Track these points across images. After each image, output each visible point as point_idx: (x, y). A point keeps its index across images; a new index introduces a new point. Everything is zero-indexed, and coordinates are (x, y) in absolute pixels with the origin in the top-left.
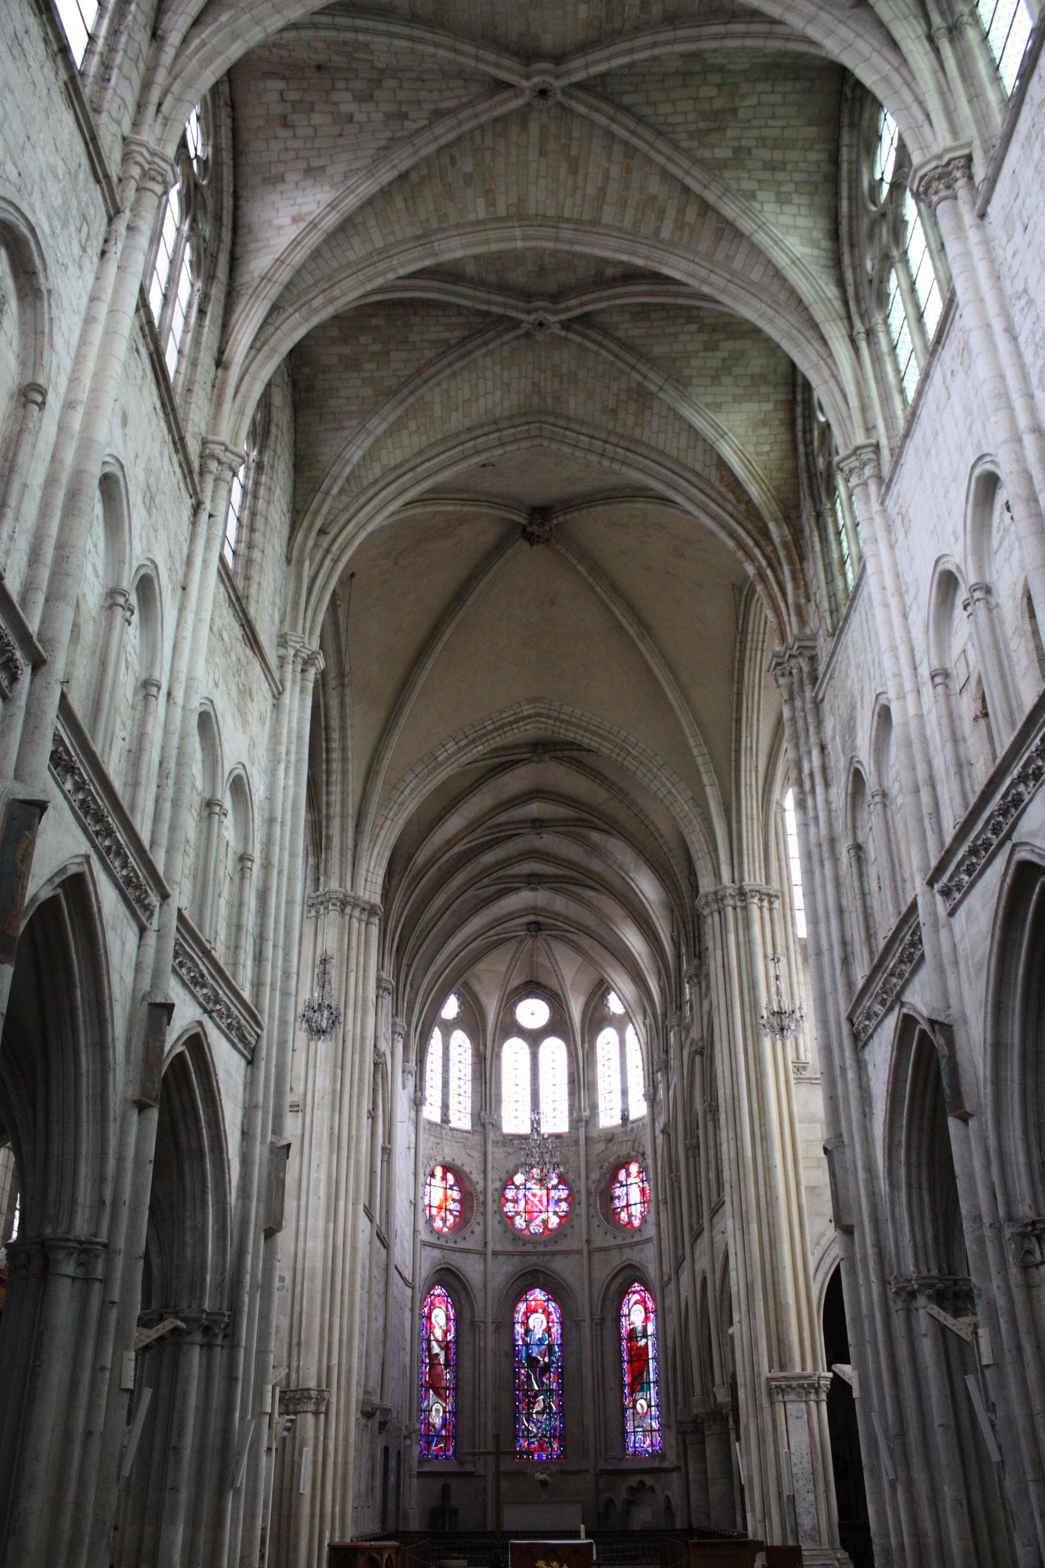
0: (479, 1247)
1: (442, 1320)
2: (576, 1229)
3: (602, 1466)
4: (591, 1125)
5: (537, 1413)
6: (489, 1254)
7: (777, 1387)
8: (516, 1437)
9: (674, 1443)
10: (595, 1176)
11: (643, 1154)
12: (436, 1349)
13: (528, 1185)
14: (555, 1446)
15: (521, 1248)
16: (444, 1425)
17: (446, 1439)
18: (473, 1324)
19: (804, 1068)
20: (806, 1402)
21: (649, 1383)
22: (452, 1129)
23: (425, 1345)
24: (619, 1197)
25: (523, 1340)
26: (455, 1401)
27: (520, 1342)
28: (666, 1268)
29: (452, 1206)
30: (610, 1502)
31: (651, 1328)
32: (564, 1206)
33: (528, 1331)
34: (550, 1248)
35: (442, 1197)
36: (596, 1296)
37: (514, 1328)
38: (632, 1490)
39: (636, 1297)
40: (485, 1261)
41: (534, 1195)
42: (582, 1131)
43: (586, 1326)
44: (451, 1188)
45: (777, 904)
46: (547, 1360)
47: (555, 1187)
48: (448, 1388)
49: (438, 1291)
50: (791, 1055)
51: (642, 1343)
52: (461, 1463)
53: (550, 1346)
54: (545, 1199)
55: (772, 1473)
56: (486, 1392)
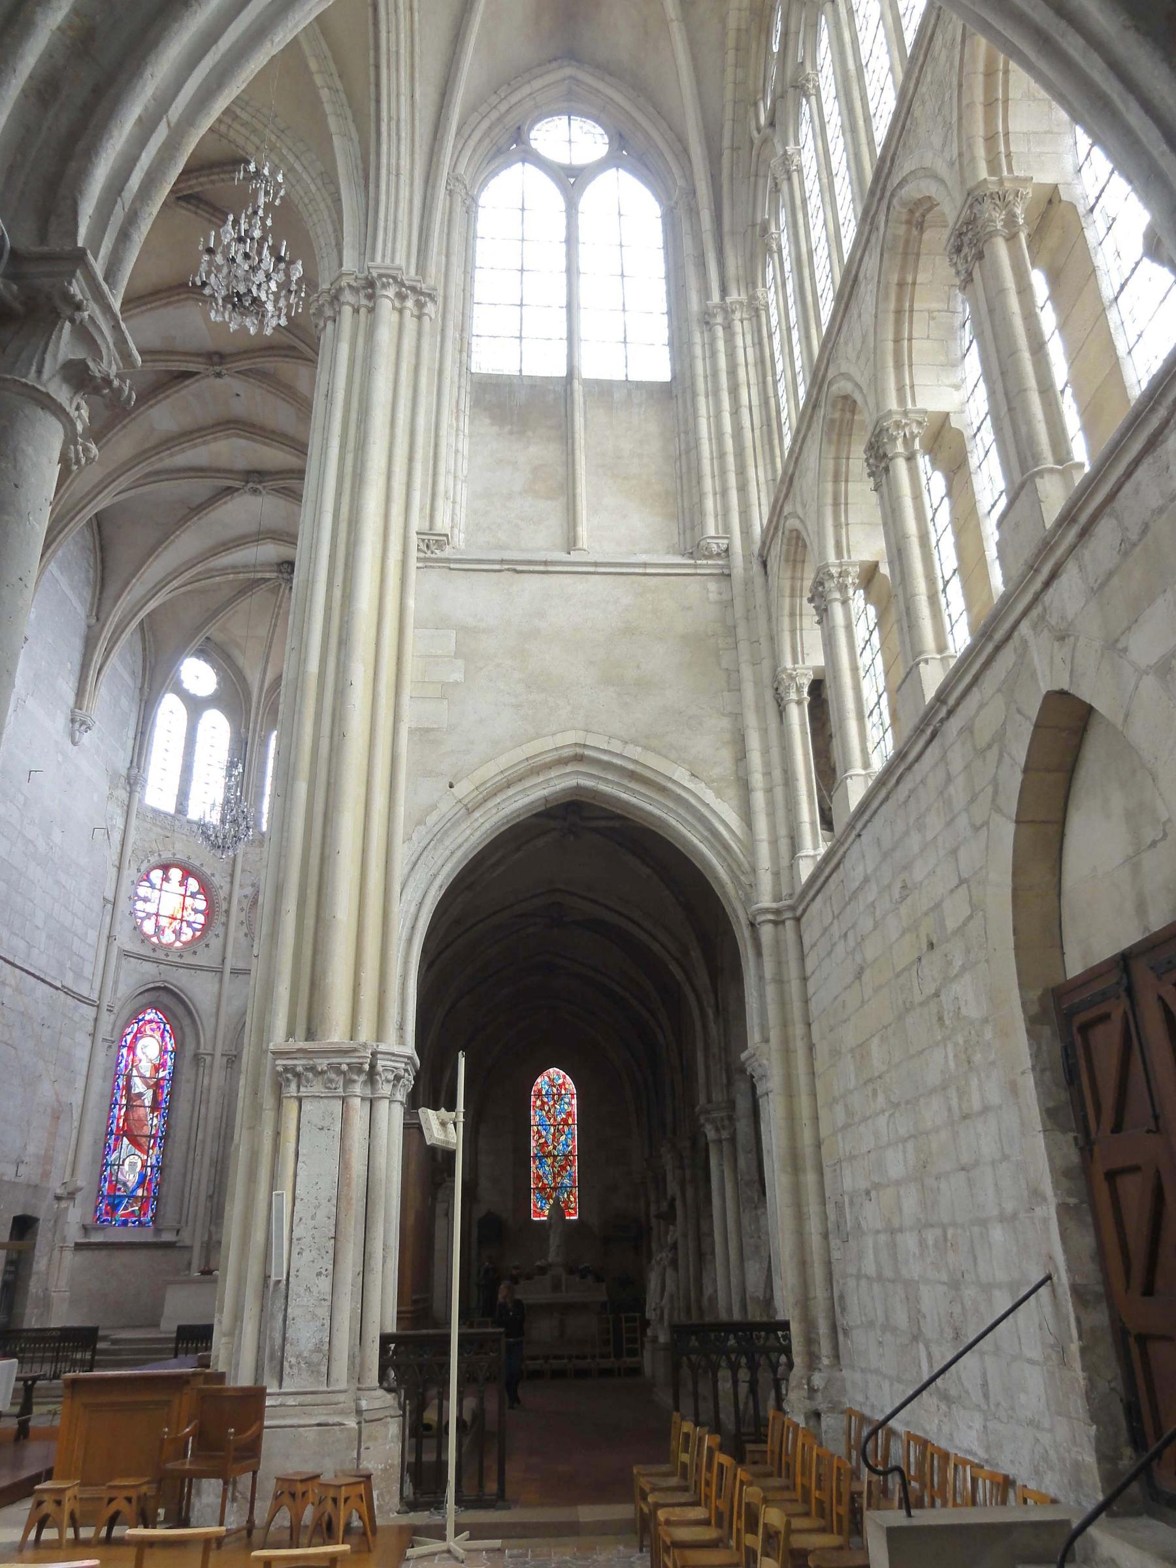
7: (286, 1069)
12: (138, 1086)
16: (141, 1182)
18: (197, 1058)
19: (440, 545)
20: (344, 1099)
22: (189, 822)
23: (122, 1082)
29: (191, 917)
35: (179, 906)
40: (221, 981)
44: (193, 896)
45: (430, 308)
48: (154, 1137)
49: (150, 1015)
50: (416, 524)
52: (158, 1231)
55: (259, 1236)
56: (204, 1141)
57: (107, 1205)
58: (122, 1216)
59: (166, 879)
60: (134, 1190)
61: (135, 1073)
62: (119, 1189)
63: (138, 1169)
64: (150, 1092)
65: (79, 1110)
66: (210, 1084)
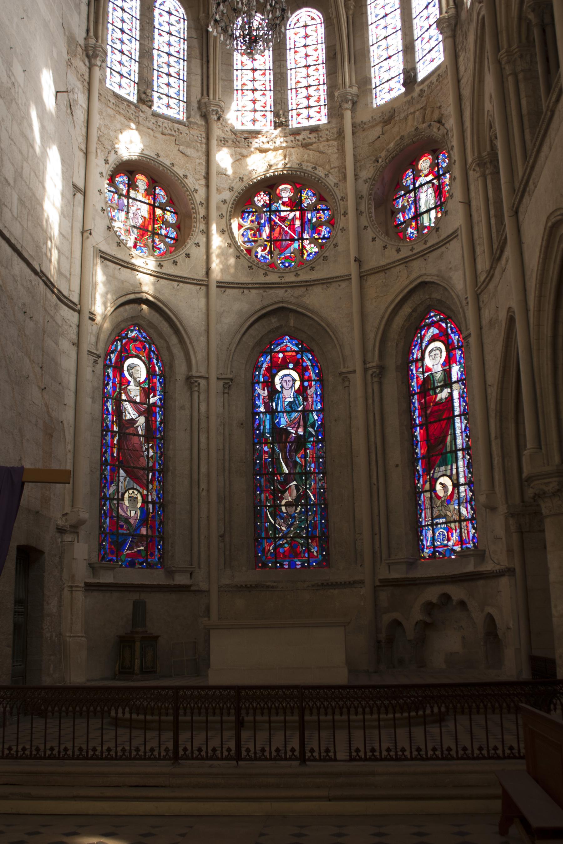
0: (200, 274)
1: (142, 374)
2: (341, 248)
3: (384, 573)
4: (360, 107)
5: (287, 505)
6: (213, 286)
8: (257, 540)
9: (500, 531)
10: (367, 173)
11: (439, 122)
12: (130, 412)
13: (274, 208)
14: (314, 550)
15: (262, 279)
17: (150, 541)
18: (190, 381)
21: (456, 450)
22: (155, 115)
24: (403, 210)
25: (266, 405)
26: (163, 488)
27: (262, 409)
28: (483, 264)
30: (397, 623)
31: (456, 371)
32: (324, 231)
33: (273, 393)
34: (304, 276)
36: (371, 336)
37: (254, 390)
38: (429, 607)
39: (433, 331)
41: (283, 219)
42: (348, 115)
43: (357, 379)
46: (301, 432)
47: (314, 209)
48: (152, 469)
51: (443, 395)
52: (170, 573)
53: (306, 413)
54: (298, 223)
56: (208, 475)
57: (111, 543)
58: (128, 555)
59: (132, 185)
60: (138, 528)
61: (124, 397)
62: (122, 526)
63: (139, 505)
64: (141, 421)
65: (72, 431)
66: (208, 411)
